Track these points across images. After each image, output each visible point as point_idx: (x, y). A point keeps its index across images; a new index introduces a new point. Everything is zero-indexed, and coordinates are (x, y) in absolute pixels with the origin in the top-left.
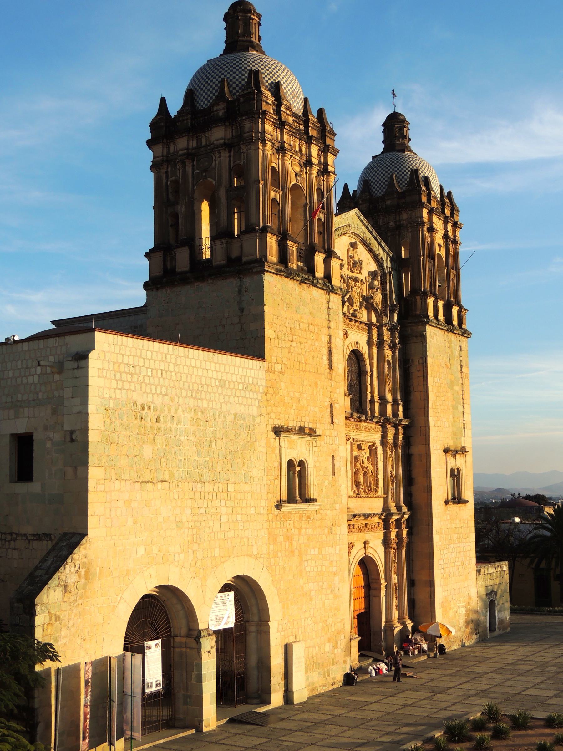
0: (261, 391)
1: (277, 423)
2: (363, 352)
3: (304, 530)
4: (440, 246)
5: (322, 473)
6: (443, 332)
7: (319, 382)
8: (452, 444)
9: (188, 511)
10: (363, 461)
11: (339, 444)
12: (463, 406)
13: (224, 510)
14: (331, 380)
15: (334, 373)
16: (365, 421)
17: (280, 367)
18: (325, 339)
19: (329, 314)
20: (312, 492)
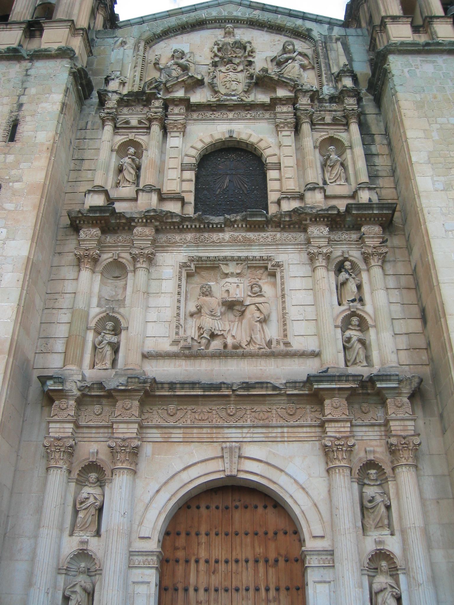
2: (253, 140)
10: (228, 291)
11: (7, 238)
14: (5, 154)
15: (16, 146)
16: (230, 224)
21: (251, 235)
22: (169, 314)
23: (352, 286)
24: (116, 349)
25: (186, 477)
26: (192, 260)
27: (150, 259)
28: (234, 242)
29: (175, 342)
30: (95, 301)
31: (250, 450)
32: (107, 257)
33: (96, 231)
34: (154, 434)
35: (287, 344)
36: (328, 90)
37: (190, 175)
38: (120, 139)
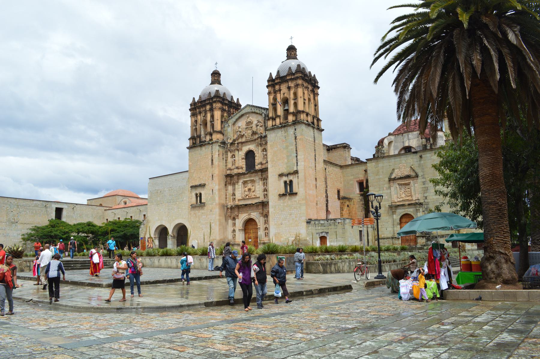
0: (187, 178)
1: (192, 185)
3: (200, 211)
4: (284, 94)
5: (207, 195)
6: (281, 129)
7: (207, 170)
8: (286, 171)
9: (167, 209)
12: (297, 154)
13: (176, 208)
15: (213, 166)
17: (193, 171)
18: (210, 158)
19: (212, 150)
20: (203, 201)
21: (251, 175)
22: (241, 192)
23: (265, 184)
24: (235, 199)
25: (245, 218)
26: (243, 181)
27: (238, 182)
28: (249, 176)
29: (242, 197)
30: (231, 191)
31: (252, 214)
32: (232, 182)
33: (229, 178)
34: (240, 212)
35: (256, 196)
36: (264, 134)
37: (244, 161)
38: (232, 154)
